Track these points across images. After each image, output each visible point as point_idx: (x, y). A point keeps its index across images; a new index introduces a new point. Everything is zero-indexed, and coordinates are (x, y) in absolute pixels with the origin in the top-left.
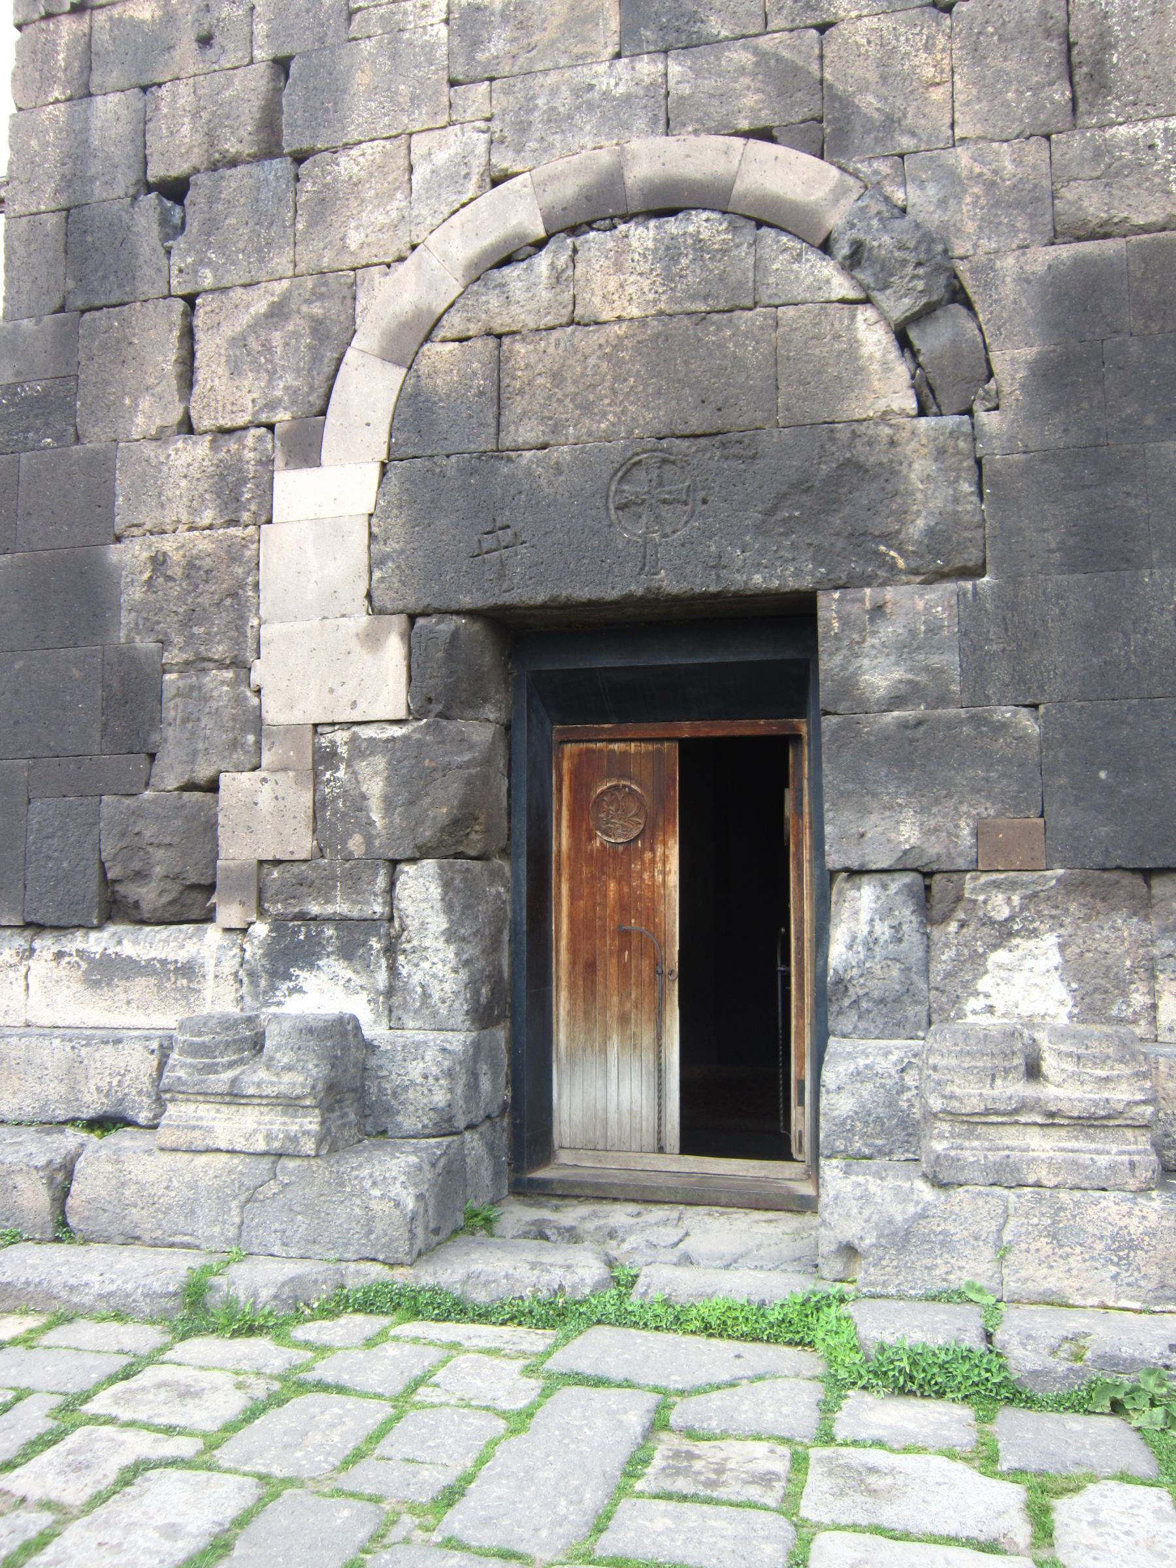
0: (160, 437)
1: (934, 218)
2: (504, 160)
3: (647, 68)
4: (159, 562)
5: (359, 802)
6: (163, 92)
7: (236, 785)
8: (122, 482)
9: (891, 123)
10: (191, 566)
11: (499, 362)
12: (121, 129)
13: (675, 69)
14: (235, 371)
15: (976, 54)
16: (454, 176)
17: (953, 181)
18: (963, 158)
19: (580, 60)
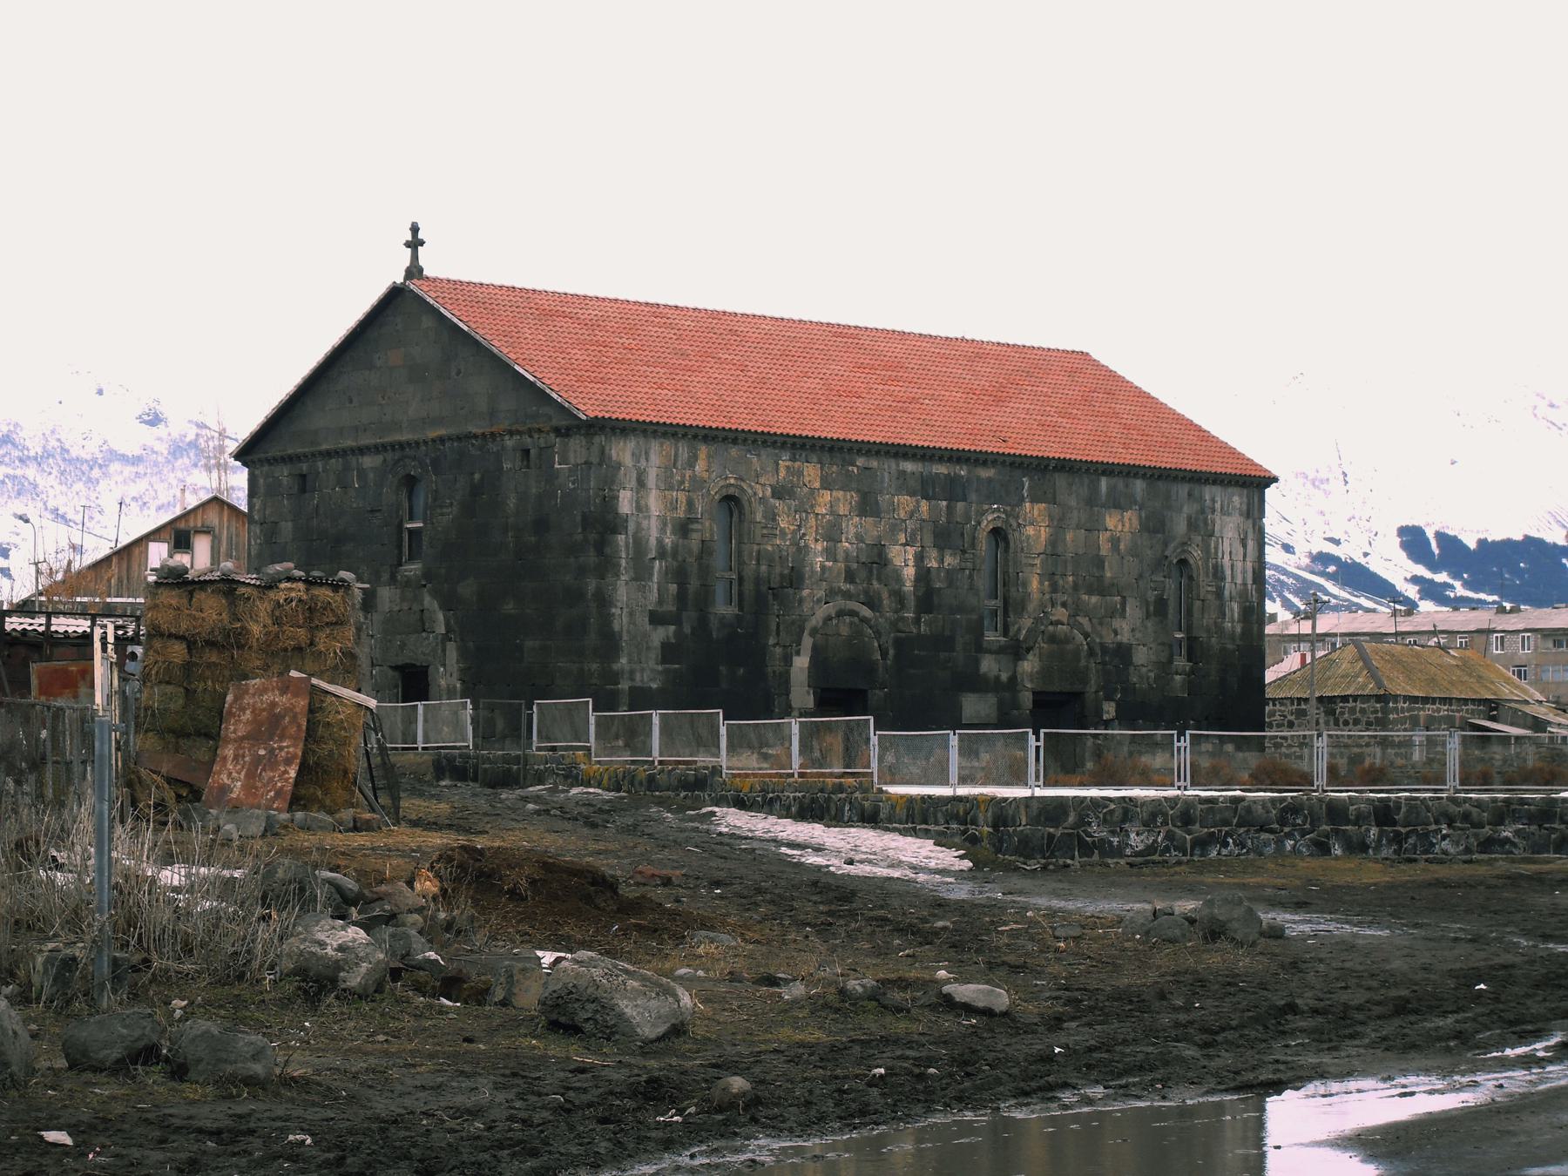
0: (775, 645)
2: (828, 599)
4: (774, 672)
16: (819, 601)
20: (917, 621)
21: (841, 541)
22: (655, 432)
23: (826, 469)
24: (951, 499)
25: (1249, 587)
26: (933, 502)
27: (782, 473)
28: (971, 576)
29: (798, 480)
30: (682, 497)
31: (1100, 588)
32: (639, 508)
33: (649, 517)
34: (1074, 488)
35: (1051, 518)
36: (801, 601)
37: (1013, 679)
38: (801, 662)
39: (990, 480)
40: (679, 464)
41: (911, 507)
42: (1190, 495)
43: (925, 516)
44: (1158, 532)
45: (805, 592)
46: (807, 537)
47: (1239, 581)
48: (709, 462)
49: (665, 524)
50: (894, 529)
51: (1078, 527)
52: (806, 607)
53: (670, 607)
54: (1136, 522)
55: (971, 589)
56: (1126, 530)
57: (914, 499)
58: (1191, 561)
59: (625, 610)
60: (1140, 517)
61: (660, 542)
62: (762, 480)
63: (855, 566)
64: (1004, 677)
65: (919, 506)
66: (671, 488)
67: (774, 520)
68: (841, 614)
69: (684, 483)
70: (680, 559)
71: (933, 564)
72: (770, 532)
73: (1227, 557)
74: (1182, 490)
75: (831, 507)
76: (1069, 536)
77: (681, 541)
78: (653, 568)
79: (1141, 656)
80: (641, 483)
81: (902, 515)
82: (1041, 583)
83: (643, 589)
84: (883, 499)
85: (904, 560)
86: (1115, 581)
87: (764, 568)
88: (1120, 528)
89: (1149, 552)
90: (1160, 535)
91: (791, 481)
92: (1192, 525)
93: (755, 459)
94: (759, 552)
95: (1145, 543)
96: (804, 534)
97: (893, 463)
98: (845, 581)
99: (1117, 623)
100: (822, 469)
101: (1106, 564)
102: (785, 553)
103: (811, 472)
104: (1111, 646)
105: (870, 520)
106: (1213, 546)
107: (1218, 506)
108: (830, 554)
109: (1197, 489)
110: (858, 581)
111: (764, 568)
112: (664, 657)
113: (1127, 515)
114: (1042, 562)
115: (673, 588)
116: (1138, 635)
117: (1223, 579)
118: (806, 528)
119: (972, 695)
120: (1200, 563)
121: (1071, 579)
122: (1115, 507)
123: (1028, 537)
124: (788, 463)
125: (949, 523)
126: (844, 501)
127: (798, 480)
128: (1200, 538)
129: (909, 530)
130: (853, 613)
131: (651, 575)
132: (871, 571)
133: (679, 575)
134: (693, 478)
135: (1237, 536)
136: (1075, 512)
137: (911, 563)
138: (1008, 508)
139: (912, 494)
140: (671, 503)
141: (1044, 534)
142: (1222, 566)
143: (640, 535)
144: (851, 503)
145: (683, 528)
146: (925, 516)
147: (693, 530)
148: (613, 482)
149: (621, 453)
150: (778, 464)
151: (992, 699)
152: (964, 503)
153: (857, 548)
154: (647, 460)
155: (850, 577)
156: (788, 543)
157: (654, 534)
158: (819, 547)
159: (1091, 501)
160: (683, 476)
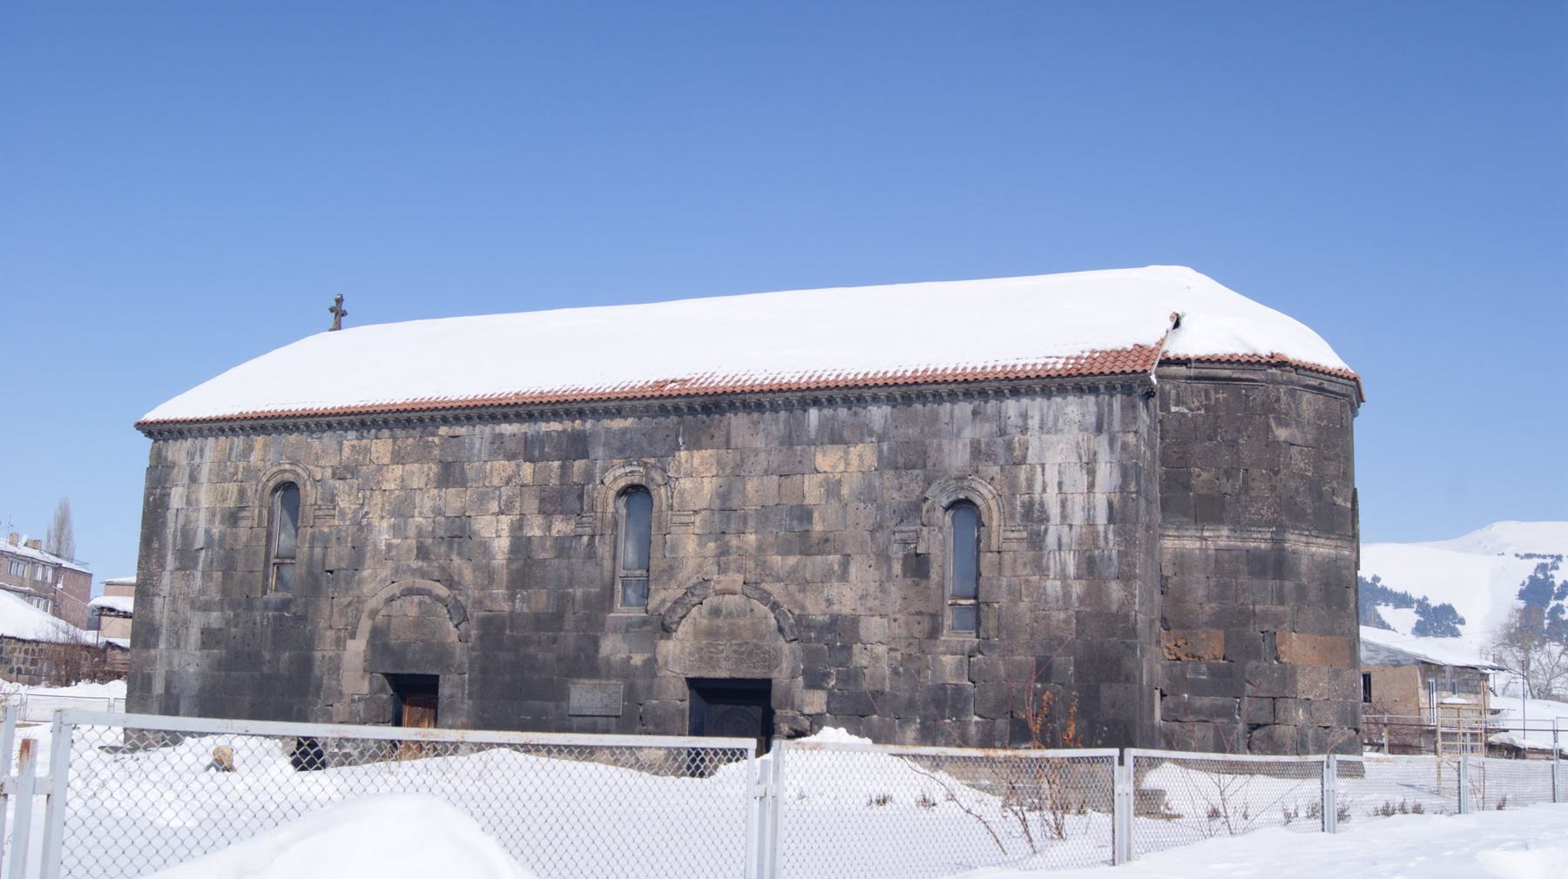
1: (464, 603)
3: (420, 563)
4: (323, 657)
5: (359, 711)
6: (329, 550)
7: (337, 705)
8: (317, 637)
9: (459, 583)
10: (330, 658)
11: (389, 624)
12: (320, 557)
13: (425, 564)
14: (341, 616)
15: (474, 571)
16: (385, 581)
17: (467, 595)
18: (470, 592)
19: (409, 559)
20: (512, 598)
21: (413, 517)
22: (200, 430)
23: (399, 442)
24: (567, 458)
25: (1101, 529)
26: (539, 464)
27: (346, 452)
29: (364, 458)
30: (233, 488)
31: (806, 545)
32: (189, 502)
33: (199, 510)
34: (762, 426)
35: (720, 464)
36: (360, 582)
37: (651, 663)
38: (357, 648)
39: (624, 432)
40: (234, 455)
41: (509, 472)
42: (975, 413)
43: (528, 479)
44: (914, 467)
45: (366, 573)
46: (371, 515)
47: (1078, 519)
48: (265, 451)
49: (214, 515)
50: (483, 498)
51: (766, 473)
52: (367, 589)
53: (214, 594)
54: (871, 459)
56: (852, 469)
57: (513, 463)
58: (978, 501)
59: (167, 599)
60: (880, 451)
61: (207, 532)
62: (322, 462)
63: (430, 541)
64: (637, 659)
66: (224, 480)
67: (333, 500)
68: (409, 592)
69: (236, 473)
70: (227, 547)
71: (537, 532)
72: (327, 512)
73: (1052, 490)
74: (964, 408)
75: (403, 480)
76: (751, 486)
77: (229, 530)
78: (197, 558)
79: (873, 628)
80: (193, 479)
81: (496, 482)
82: (702, 545)
83: (188, 578)
84: (470, 470)
85: (495, 532)
86: (831, 536)
87: (318, 551)
89: (895, 495)
90: (916, 472)
91: (357, 460)
92: (977, 451)
93: (316, 444)
94: (313, 537)
95: (887, 484)
96: (367, 513)
97: (487, 430)
98: (418, 557)
99: (834, 589)
100: (394, 444)
101: (816, 515)
102: (343, 534)
103: (381, 447)
104: (821, 618)
105: (452, 491)
106: (1023, 476)
107: (1034, 423)
108: (397, 530)
109: (992, 405)
110: (433, 557)
111: (318, 551)
112: (203, 643)
113: (854, 451)
114: (704, 520)
115: (218, 575)
116: (871, 602)
117: (1044, 519)
118: (370, 506)
119: (587, 682)
120: (993, 503)
121: (751, 538)
122: (833, 442)
123: (682, 493)
124: (355, 442)
125: (561, 484)
126: (419, 474)
127: (364, 458)
128: (997, 469)
129: (504, 498)
130: (420, 592)
131: (196, 564)
132: (450, 546)
133: (228, 563)
134: (247, 469)
135: (1073, 459)
136: (763, 456)
137: (505, 533)
138: (652, 461)
139: (511, 457)
140: (222, 495)
141: (709, 486)
142: (1042, 504)
143: (187, 527)
144: (428, 475)
145: (233, 518)
146: (528, 479)
147: (243, 518)
148: (166, 480)
149: (176, 454)
150: (341, 444)
151: (617, 686)
152: (584, 461)
153: (434, 522)
154: (202, 456)
155: (423, 552)
156: (348, 523)
157: (202, 525)
158: (385, 524)
159: (790, 440)
160: (237, 467)
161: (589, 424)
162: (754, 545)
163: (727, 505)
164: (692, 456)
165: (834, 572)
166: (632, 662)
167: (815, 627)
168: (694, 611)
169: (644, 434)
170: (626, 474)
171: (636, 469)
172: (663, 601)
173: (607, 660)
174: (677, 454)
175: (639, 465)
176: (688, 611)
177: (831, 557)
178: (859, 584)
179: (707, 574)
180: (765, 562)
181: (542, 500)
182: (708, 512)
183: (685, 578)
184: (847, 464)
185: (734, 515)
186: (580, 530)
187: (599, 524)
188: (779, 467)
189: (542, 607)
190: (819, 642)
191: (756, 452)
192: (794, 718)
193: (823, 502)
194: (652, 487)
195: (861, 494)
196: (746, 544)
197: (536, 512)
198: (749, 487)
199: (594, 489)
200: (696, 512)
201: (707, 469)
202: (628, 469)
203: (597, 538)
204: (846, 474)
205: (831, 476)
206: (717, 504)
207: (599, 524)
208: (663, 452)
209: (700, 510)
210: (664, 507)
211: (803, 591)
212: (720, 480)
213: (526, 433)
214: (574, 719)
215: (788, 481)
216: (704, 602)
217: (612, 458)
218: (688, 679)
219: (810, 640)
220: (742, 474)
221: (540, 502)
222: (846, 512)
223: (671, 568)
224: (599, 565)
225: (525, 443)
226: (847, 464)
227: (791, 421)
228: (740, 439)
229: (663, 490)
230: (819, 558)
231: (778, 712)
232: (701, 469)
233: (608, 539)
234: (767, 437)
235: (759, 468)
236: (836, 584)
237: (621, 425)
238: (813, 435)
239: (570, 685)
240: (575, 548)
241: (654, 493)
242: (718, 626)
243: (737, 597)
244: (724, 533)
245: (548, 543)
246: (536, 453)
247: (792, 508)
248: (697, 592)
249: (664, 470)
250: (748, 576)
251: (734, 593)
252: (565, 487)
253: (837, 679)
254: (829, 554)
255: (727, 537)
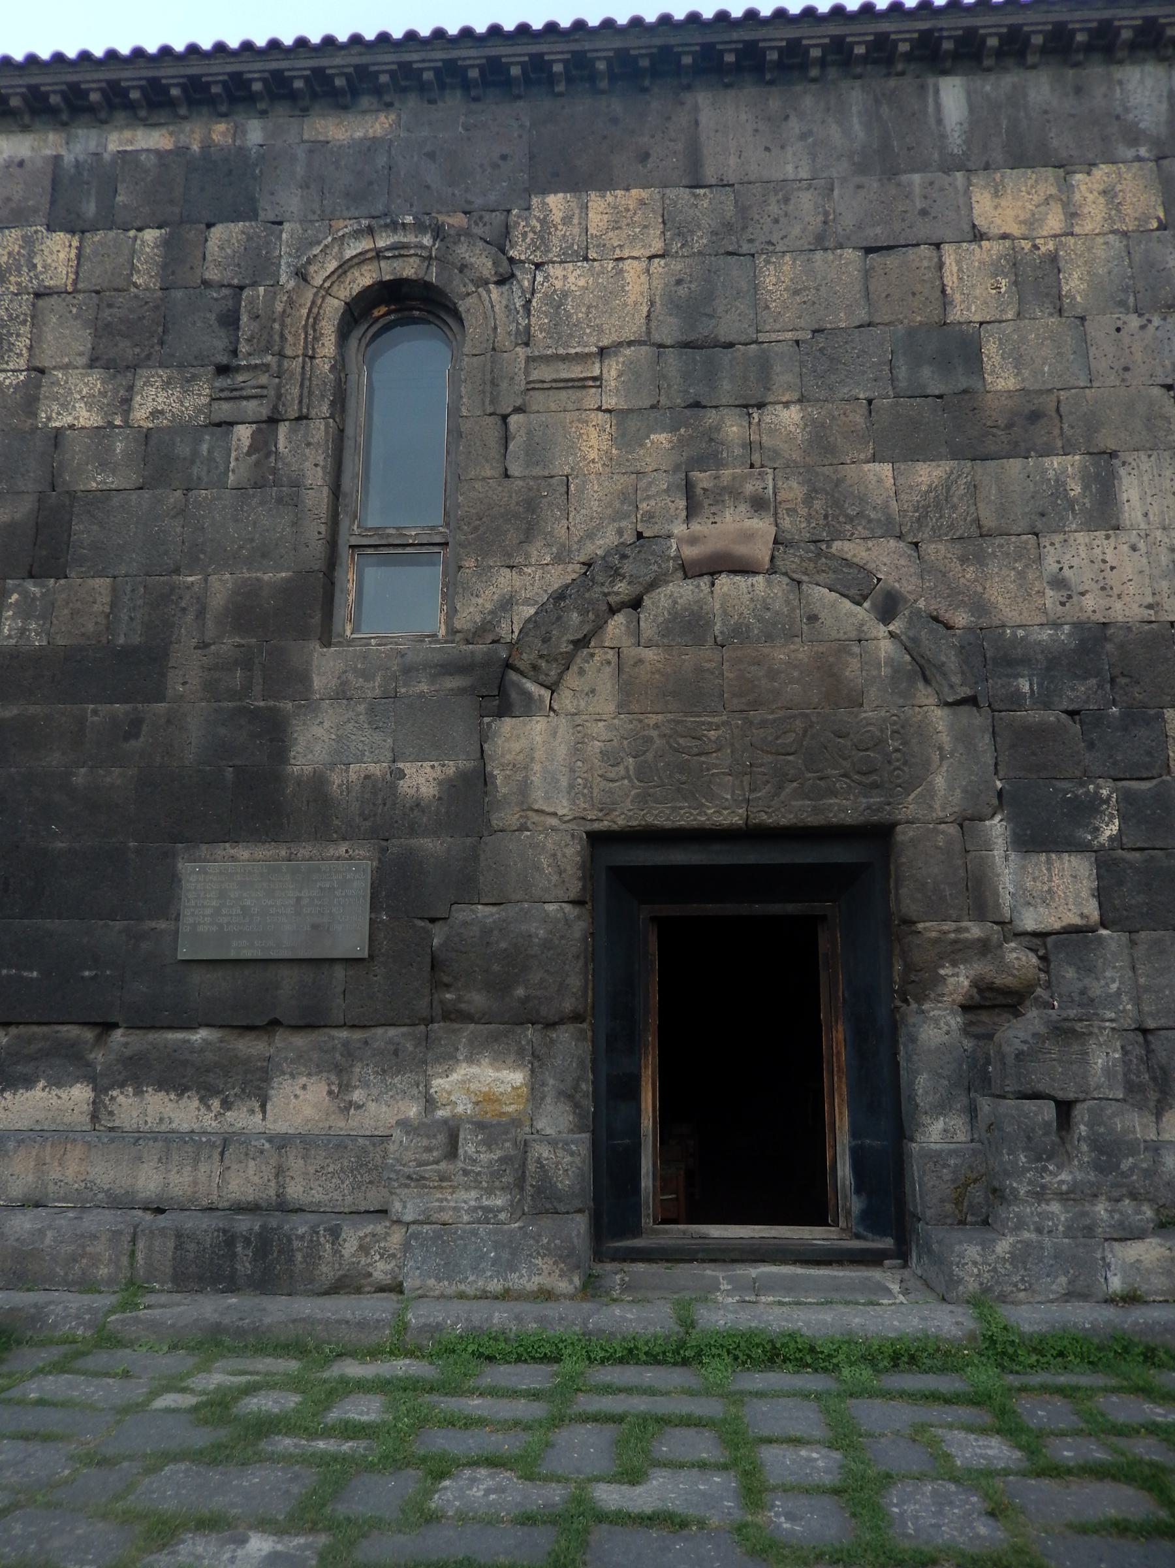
26: (99, 236)
28: (263, 444)
34: (795, 126)
39: (370, 147)
51: (820, 242)
55: (259, 485)
56: (1087, 226)
65: (31, 254)
71: (85, 417)
88: (1054, 222)
101: (991, 349)
104: (1046, 634)
119: (243, 852)
121: (790, 417)
123: (558, 301)
136: (806, 201)
138: (458, 220)
161: (255, 133)
162: (800, 436)
163: (704, 329)
164: (585, 208)
165: (1071, 504)
166: (404, 786)
167: (1026, 661)
168: (617, 626)
169: (431, 156)
170: (379, 255)
171: (410, 238)
172: (507, 604)
173: (318, 782)
174: (535, 201)
175: (420, 227)
176: (598, 628)
177: (1056, 461)
178: (1158, 533)
179: (650, 517)
180: (838, 483)
181: (103, 331)
182: (644, 349)
183: (577, 533)
184: (1072, 215)
185: (725, 356)
186: (225, 410)
187: (293, 391)
188: (859, 227)
189: (90, 627)
190: (1047, 706)
191: (783, 189)
192: (984, 947)
193: (1010, 315)
194: (457, 286)
195: (1125, 290)
196: (771, 432)
197: (82, 361)
198: (769, 279)
199: (271, 297)
200: (602, 352)
201: (633, 240)
202: (383, 241)
203: (283, 429)
204: (1071, 240)
205: (1026, 245)
206: (669, 330)
207: (293, 391)
208: (492, 197)
209: (620, 344)
210: (504, 339)
211: (980, 559)
212: (677, 266)
213: (57, 159)
214: (197, 977)
215: (891, 261)
216: (647, 601)
217: (327, 217)
218: (588, 834)
219: (1016, 700)
220: (745, 248)
221: (97, 336)
222: (1084, 338)
223: (531, 505)
224: (295, 502)
225: (55, 182)
226: (1072, 215)
227: (885, 110)
228: (733, 161)
229: (495, 291)
230: (1014, 466)
231: (930, 928)
232: (614, 239)
233: (319, 430)
234: (813, 157)
235: (796, 231)
236: (1082, 537)
237: (359, 134)
238: (955, 141)
239: (184, 867)
240: (211, 459)
241: (462, 307)
242: (699, 670)
243: (760, 579)
244: (697, 405)
245: (119, 447)
246: (90, 209)
247: (911, 332)
248: (627, 568)
249: (500, 243)
250: (786, 523)
251: (744, 569)
252: (179, 294)
253: (1123, 818)
254: (1048, 452)
255: (711, 417)
